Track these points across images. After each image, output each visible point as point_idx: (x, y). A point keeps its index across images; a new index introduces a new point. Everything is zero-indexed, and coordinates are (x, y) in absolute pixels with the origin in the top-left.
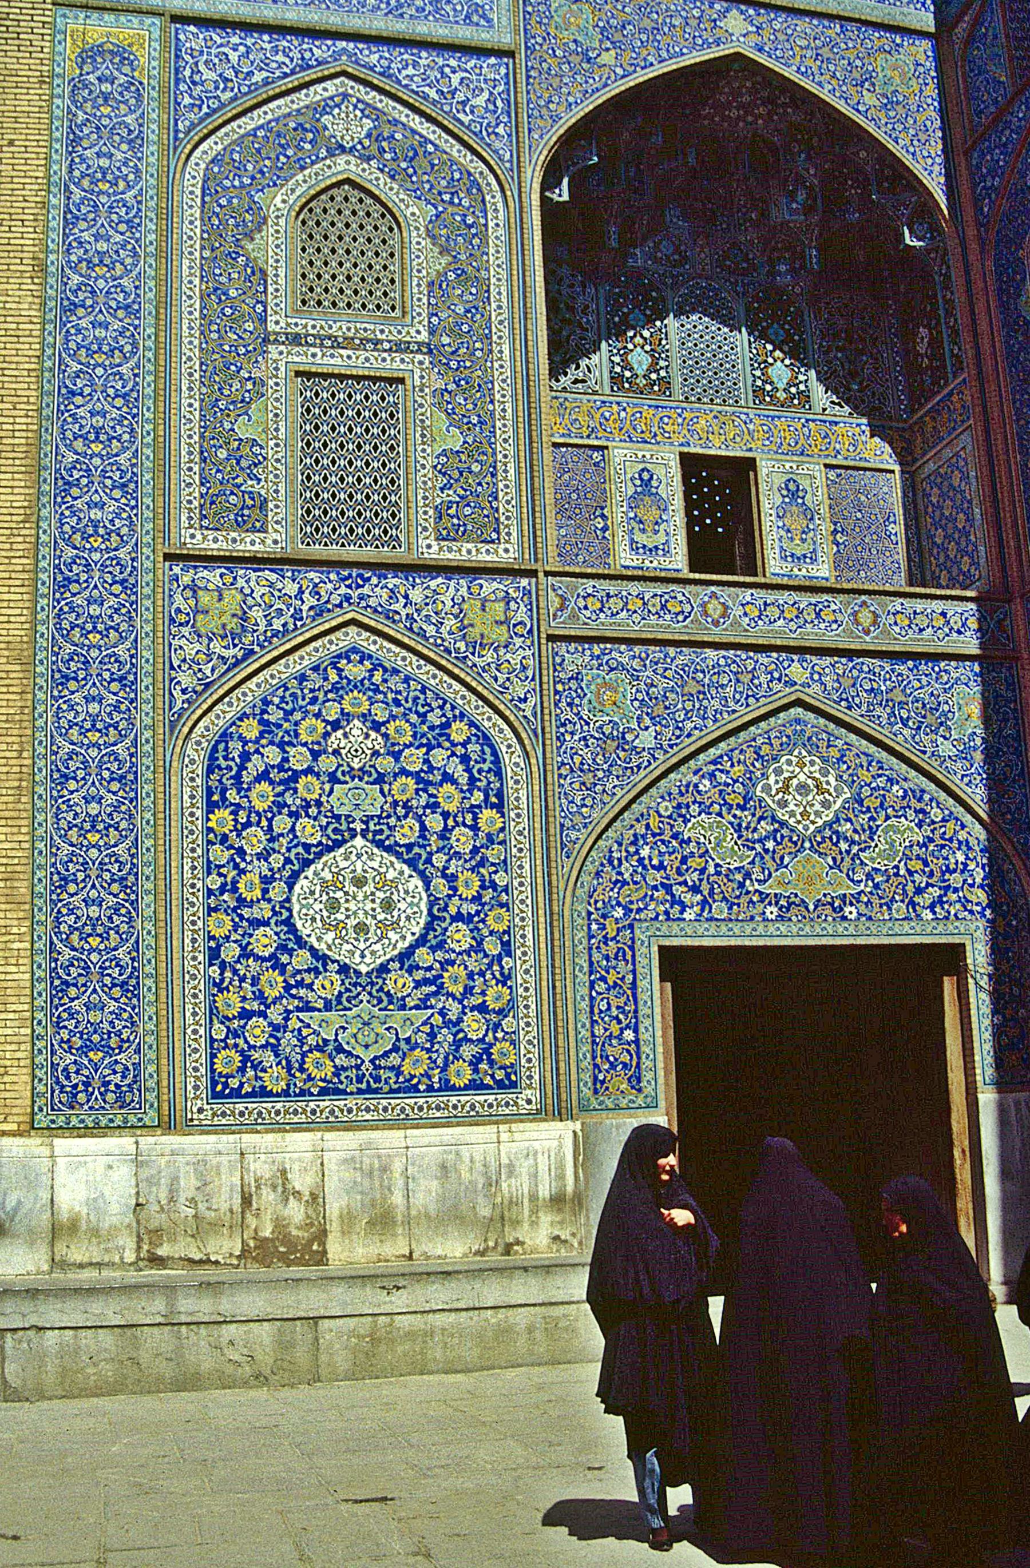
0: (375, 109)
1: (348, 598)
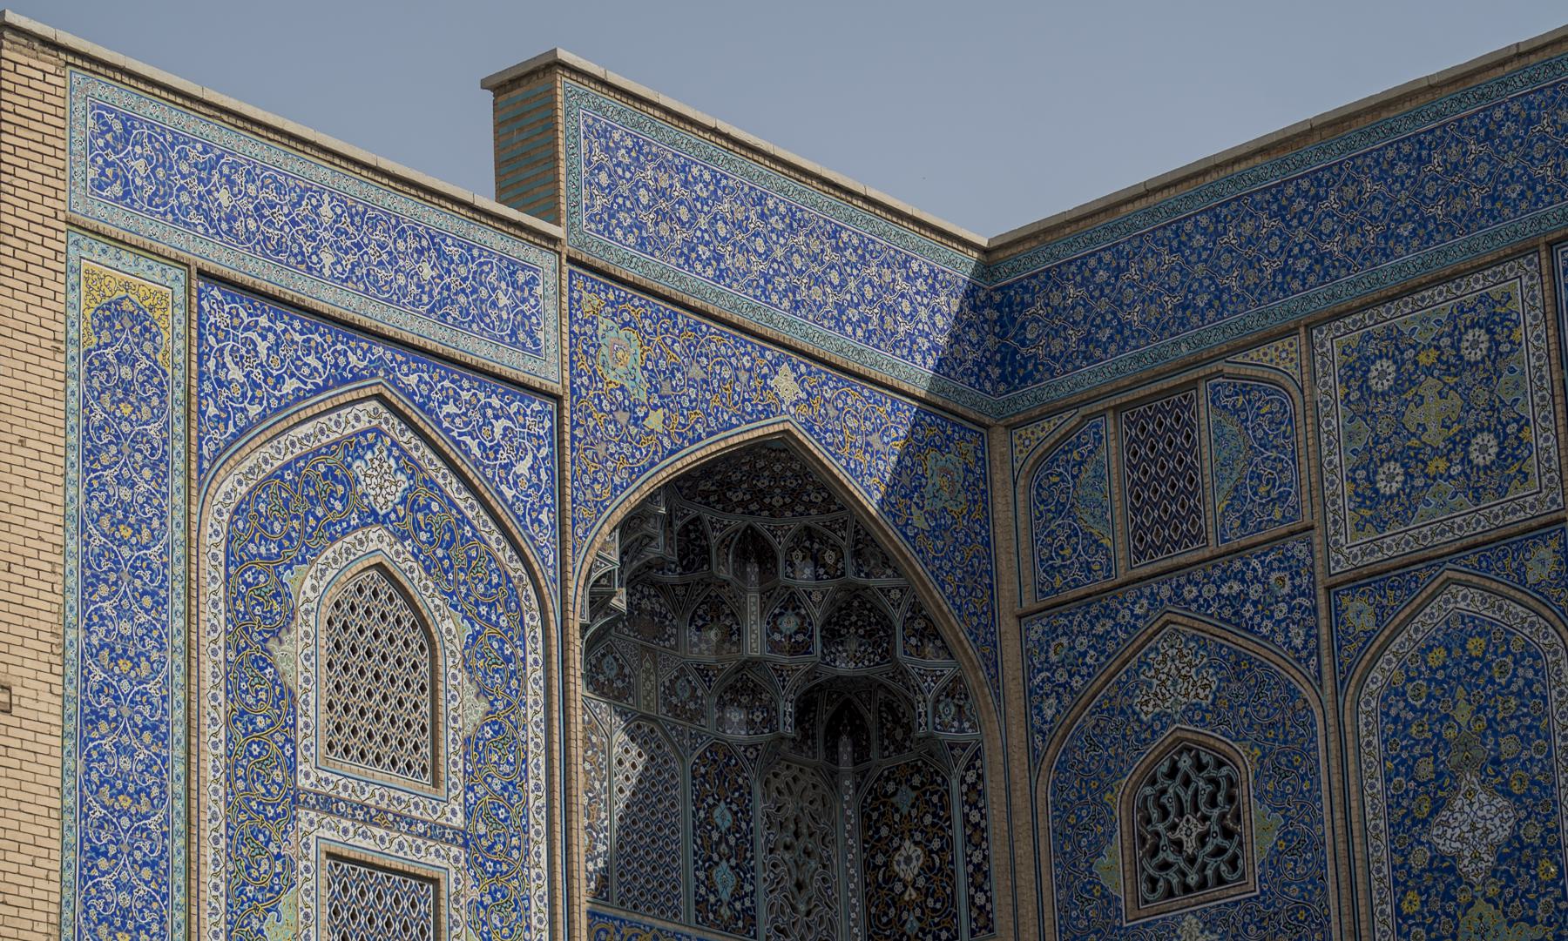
0: (411, 459)
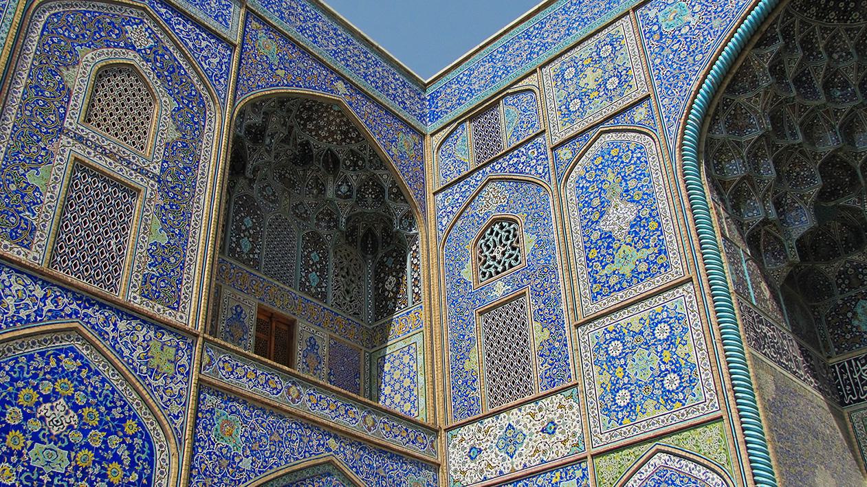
1: (76, 313)
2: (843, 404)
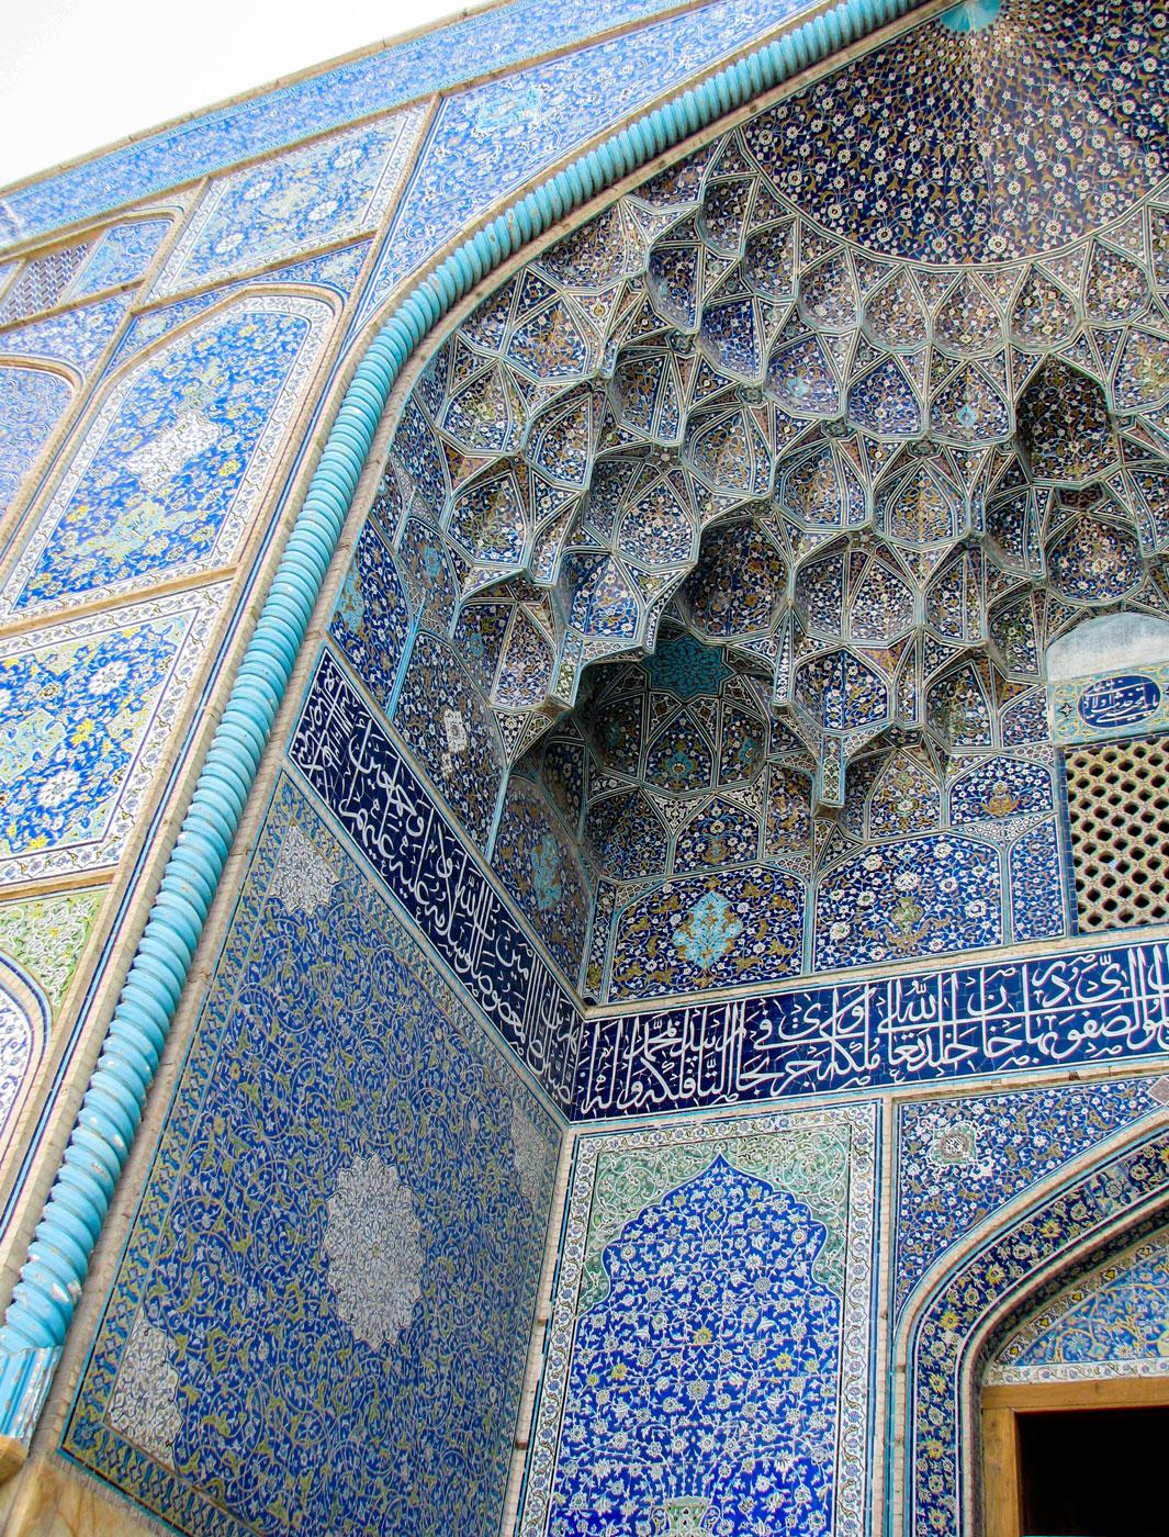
2: (573, 1113)
